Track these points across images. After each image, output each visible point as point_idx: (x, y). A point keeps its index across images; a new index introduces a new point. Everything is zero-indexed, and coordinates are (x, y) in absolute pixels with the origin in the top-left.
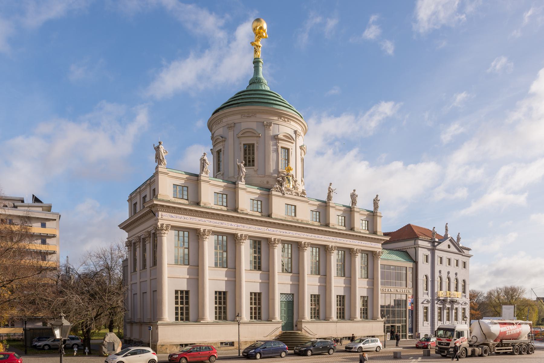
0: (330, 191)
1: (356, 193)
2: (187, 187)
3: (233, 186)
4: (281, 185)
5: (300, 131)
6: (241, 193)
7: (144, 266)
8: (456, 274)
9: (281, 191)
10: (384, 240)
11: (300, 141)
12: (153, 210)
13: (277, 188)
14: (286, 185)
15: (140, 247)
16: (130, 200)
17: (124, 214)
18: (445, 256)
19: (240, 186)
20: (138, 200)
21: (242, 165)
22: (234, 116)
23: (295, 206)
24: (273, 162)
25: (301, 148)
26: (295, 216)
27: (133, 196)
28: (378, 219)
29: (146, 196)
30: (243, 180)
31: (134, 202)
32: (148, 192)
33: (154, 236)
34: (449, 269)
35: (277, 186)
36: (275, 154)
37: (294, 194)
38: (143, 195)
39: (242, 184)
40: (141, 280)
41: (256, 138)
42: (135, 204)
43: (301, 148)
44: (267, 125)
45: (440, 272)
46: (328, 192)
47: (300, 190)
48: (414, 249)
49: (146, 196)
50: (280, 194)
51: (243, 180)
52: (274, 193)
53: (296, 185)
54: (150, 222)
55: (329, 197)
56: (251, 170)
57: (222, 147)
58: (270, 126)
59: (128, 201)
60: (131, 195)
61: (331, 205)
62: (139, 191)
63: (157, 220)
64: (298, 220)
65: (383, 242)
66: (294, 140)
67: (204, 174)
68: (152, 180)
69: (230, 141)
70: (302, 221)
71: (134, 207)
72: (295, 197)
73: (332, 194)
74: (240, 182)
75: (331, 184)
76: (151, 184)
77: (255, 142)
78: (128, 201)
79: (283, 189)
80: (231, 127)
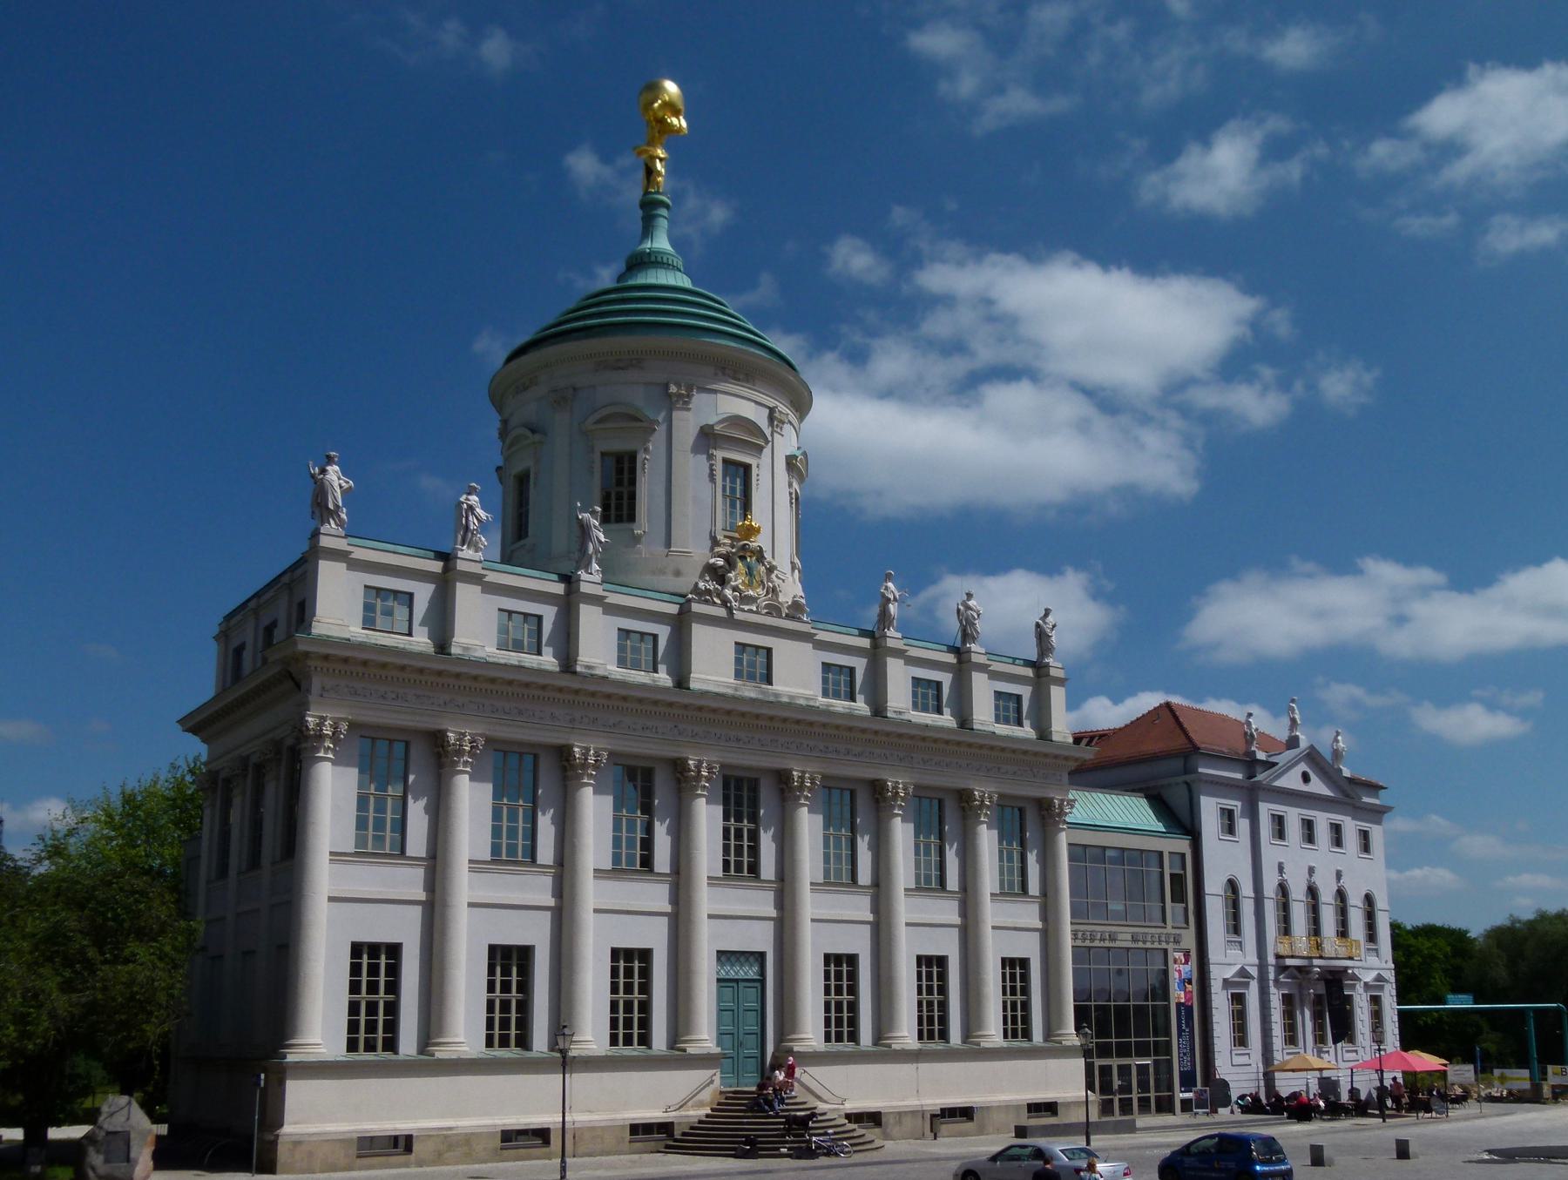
8: (1339, 875)
9: (725, 603)
13: (708, 592)
16: (224, 636)
17: (200, 683)
19: (585, 588)
20: (249, 635)
27: (233, 621)
29: (274, 624)
31: (235, 643)
32: (281, 611)
38: (266, 621)
42: (239, 651)
45: (1281, 868)
51: (595, 567)
59: (216, 638)
60: (228, 618)
63: (304, 707)
64: (777, 695)
70: (791, 697)
71: (233, 663)
72: (769, 621)
78: (216, 638)
79: (728, 592)
80: (563, 398)
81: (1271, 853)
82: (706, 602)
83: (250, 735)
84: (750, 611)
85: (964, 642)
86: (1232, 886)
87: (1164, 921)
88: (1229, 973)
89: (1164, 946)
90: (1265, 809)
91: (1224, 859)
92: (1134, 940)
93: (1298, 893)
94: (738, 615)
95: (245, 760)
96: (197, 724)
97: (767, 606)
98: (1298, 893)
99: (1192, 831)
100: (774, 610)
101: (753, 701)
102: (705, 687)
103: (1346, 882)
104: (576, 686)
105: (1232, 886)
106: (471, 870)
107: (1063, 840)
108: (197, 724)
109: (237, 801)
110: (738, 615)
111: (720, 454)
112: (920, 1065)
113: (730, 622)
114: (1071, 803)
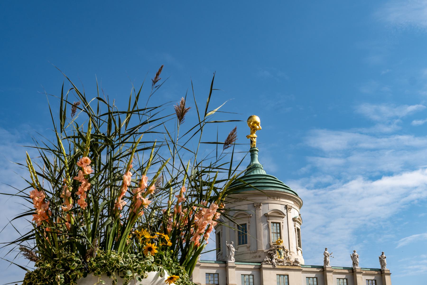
1: (356, 254)
3: (224, 265)
4: (272, 258)
6: (231, 271)
9: (272, 264)
11: (294, 213)
13: (268, 261)
14: (276, 256)
19: (230, 265)
21: (231, 245)
23: (288, 275)
24: (264, 238)
25: (294, 220)
30: (233, 258)
35: (268, 259)
36: (266, 231)
37: (286, 264)
39: (232, 262)
41: (247, 219)
43: (294, 220)
46: (324, 256)
47: (292, 260)
50: (271, 266)
51: (233, 258)
52: (264, 266)
53: (287, 255)
55: (326, 262)
56: (243, 248)
57: (220, 230)
58: (260, 205)
61: (327, 269)
66: (284, 215)
72: (288, 267)
73: (328, 259)
74: (229, 261)
75: (326, 249)
77: (247, 222)
82: (267, 264)
84: (281, 265)
85: (354, 266)
94: (277, 267)
97: (286, 263)
100: (289, 263)
110: (277, 267)
111: (270, 221)
113: (274, 268)
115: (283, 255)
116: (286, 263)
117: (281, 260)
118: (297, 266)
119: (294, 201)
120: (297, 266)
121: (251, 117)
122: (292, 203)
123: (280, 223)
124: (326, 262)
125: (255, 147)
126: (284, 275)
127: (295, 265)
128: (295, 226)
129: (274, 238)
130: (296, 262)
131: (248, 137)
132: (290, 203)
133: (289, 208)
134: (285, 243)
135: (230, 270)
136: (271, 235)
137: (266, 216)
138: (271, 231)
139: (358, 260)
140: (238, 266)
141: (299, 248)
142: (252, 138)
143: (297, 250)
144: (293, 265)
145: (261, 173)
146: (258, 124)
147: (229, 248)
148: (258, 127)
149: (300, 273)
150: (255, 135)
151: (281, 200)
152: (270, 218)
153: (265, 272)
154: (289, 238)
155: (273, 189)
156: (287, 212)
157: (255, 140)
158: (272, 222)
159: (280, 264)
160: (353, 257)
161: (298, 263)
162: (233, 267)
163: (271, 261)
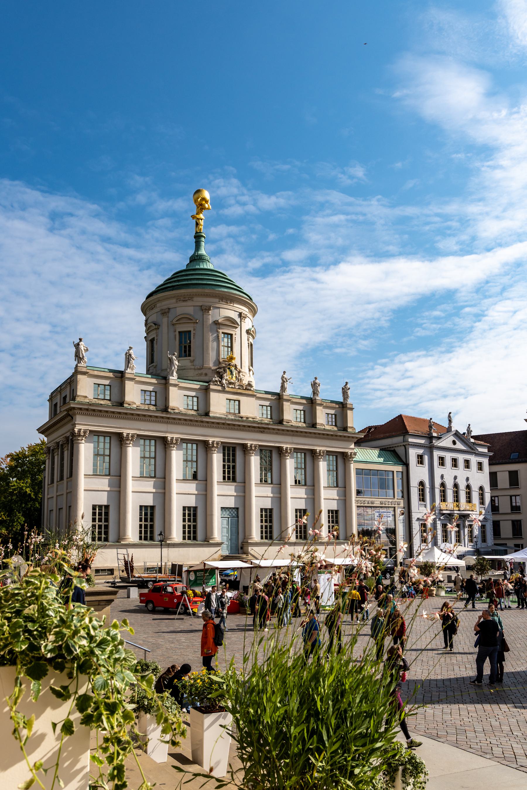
0: (284, 381)
1: (317, 381)
2: (110, 386)
3: (163, 381)
4: (221, 377)
5: (246, 313)
6: (173, 391)
7: (62, 478)
8: (468, 479)
9: (222, 385)
10: (357, 438)
11: (247, 324)
12: (70, 413)
13: (216, 381)
14: (227, 376)
15: (58, 454)
16: (51, 400)
17: (43, 416)
18: (448, 456)
19: (171, 382)
20: (58, 400)
21: (174, 357)
22: (167, 301)
23: (239, 401)
24: (213, 352)
25: (248, 332)
26: (239, 413)
27: (54, 395)
28: (349, 412)
29: (66, 396)
30: (175, 374)
31: (54, 403)
32: (67, 392)
33: (70, 443)
34: (455, 472)
35: (217, 379)
36: (215, 344)
37: (237, 387)
38: (63, 395)
39: (173, 378)
40: (58, 494)
41: (192, 325)
42: (56, 405)
43: (248, 332)
44: (206, 309)
45: (442, 477)
46: (281, 381)
47: (245, 382)
48: (403, 448)
49: (66, 396)
50: (220, 388)
51: (175, 374)
52: (212, 387)
53: (239, 376)
54: (68, 427)
55: (283, 388)
56: (186, 362)
57: (155, 336)
58: (209, 309)
60: (52, 393)
61: (285, 397)
62: (59, 390)
63: (74, 425)
65: (356, 440)
66: (238, 324)
67: (129, 371)
68: (72, 379)
69: (164, 328)
71: (54, 410)
74: (171, 378)
75: (284, 372)
76: (71, 383)
77: (191, 329)
79: (224, 381)
80: (165, 312)
81: (438, 471)
82: (216, 385)
83: (59, 434)
84: (232, 388)
85: (314, 395)
86: (422, 484)
87: (394, 497)
88: (420, 516)
89: (393, 506)
90: (437, 454)
91: (419, 473)
92: (381, 503)
93: (449, 485)
94: (227, 389)
95: (58, 443)
96: (43, 430)
97: (238, 385)
98: (449, 485)
99: (406, 465)
101: (232, 420)
102: (215, 415)
103: (471, 482)
104: (168, 416)
105: (422, 484)
106: (133, 480)
107: (353, 467)
108: (43, 430)
109: (56, 457)
110: (227, 389)
111: (221, 331)
112: (296, 547)
113: (223, 391)
114: (355, 454)
115: (235, 375)
116: (238, 385)
117: (232, 381)
118: (250, 390)
119: (249, 309)
120: (250, 390)
121: (198, 191)
122: (247, 310)
123: (231, 335)
124: (283, 388)
125: (201, 232)
126: (235, 400)
127: (248, 389)
128: (248, 340)
129: (224, 354)
130: (250, 385)
131: (193, 217)
132: (245, 310)
133: (244, 317)
134: (236, 361)
135: (171, 389)
136: (222, 348)
137: (216, 323)
138: (222, 344)
139: (319, 389)
140: (181, 385)
141: (251, 368)
142: (198, 219)
143: (250, 370)
144: (246, 389)
145: (209, 268)
146: (207, 202)
147: (171, 360)
148: (207, 206)
149: (253, 399)
150: (201, 216)
151: (235, 305)
152: (221, 326)
153: (213, 395)
154: (241, 355)
155: (226, 290)
156: (241, 321)
157: (202, 222)
158: (223, 333)
159: (230, 386)
160: (314, 385)
161: (252, 387)
162: (175, 385)
163: (220, 382)
